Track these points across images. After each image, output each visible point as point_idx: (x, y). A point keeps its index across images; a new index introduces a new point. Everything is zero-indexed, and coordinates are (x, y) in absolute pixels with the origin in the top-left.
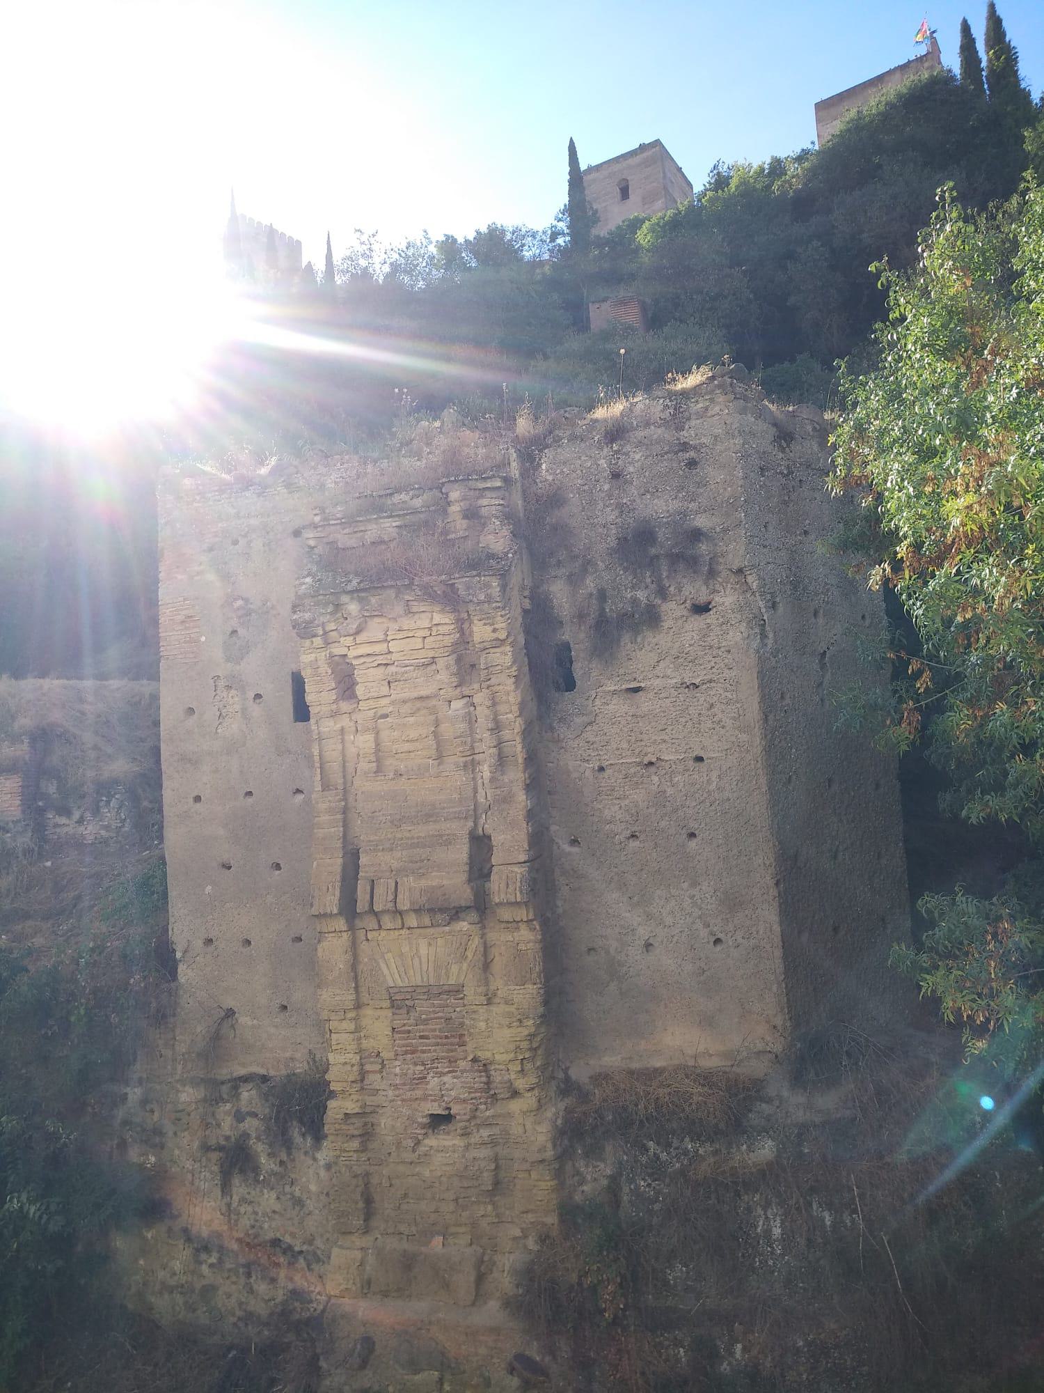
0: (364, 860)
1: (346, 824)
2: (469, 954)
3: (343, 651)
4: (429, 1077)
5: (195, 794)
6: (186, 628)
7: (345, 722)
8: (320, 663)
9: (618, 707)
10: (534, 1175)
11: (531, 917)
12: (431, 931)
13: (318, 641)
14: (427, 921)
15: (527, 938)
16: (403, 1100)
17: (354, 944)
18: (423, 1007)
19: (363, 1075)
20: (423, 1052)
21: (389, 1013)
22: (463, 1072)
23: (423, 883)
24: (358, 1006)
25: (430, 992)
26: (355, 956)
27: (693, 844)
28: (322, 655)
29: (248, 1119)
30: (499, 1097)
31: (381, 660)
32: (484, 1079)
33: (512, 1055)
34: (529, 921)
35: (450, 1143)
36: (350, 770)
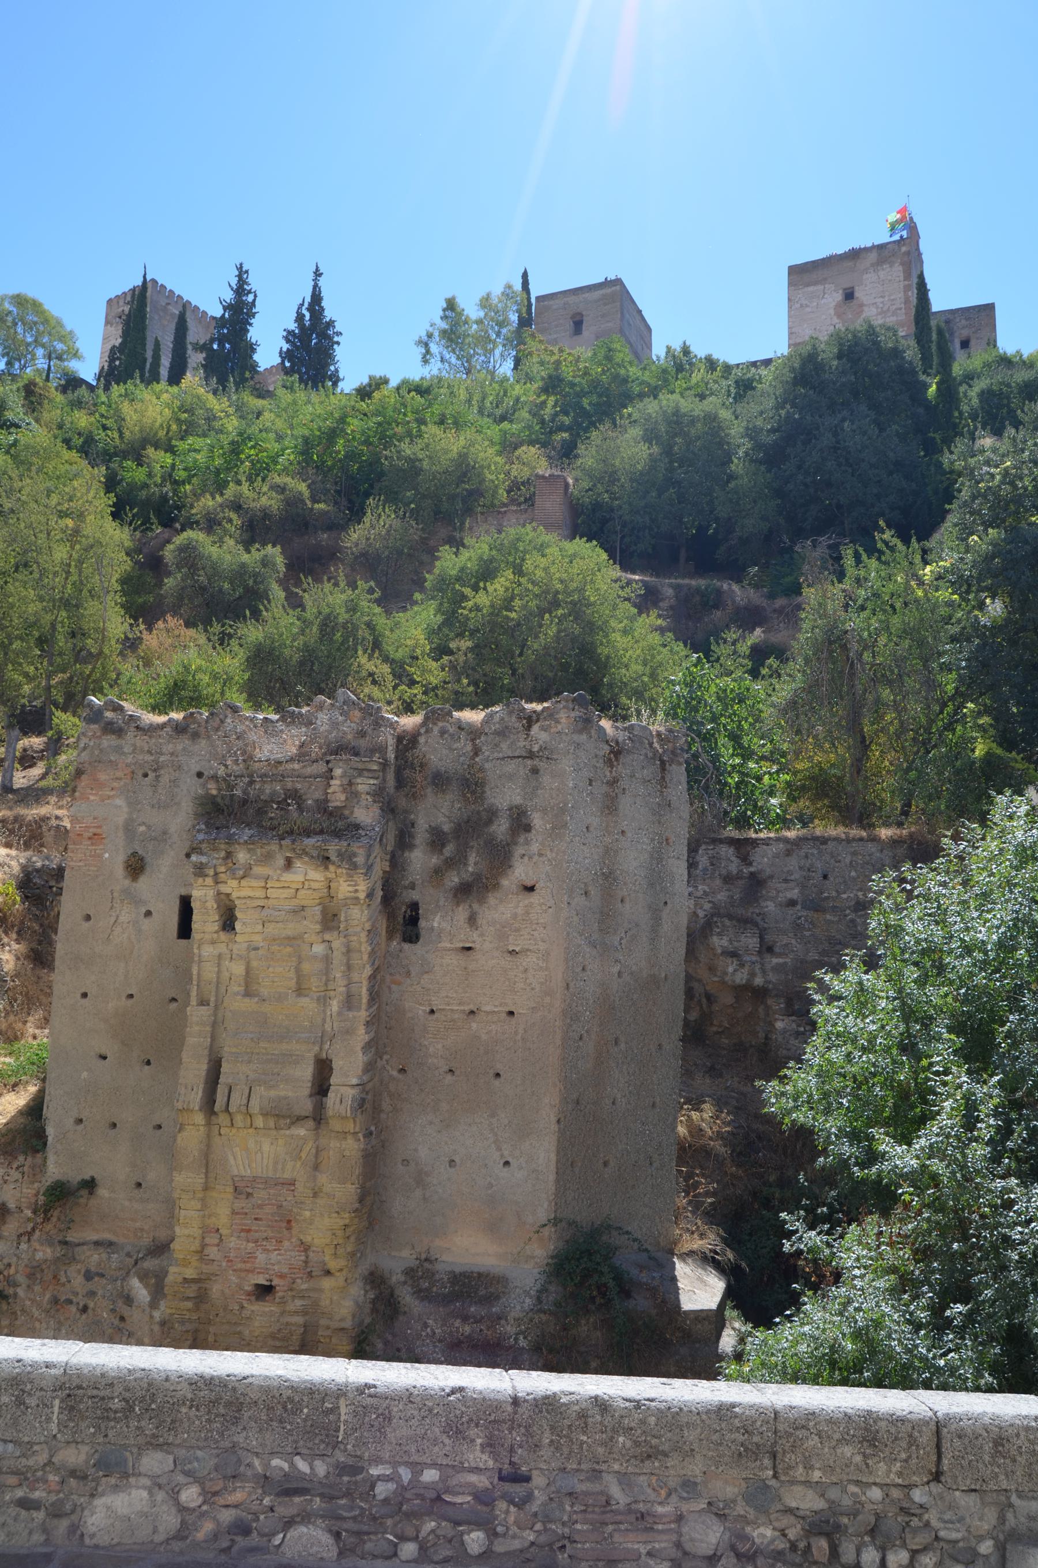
0: (225, 1068)
1: (213, 1038)
2: (303, 1155)
3: (228, 890)
4: (258, 1253)
5: (83, 990)
6: (92, 844)
7: (222, 948)
8: (208, 898)
9: (452, 961)
10: (334, 1340)
11: (357, 1130)
12: (274, 1132)
13: (209, 881)
14: (271, 1123)
15: (352, 1147)
16: (234, 1270)
17: (209, 1136)
18: (260, 1195)
19: (204, 1246)
20: (256, 1231)
21: (230, 1197)
22: (286, 1251)
23: (273, 1093)
24: (206, 1188)
25: (268, 1183)
26: (209, 1146)
27: (497, 1083)
28: (211, 893)
29: (96, 1279)
30: (314, 1274)
31: (261, 903)
32: (303, 1258)
33: (328, 1241)
34: (355, 1133)
35: (267, 1309)
36: (223, 990)
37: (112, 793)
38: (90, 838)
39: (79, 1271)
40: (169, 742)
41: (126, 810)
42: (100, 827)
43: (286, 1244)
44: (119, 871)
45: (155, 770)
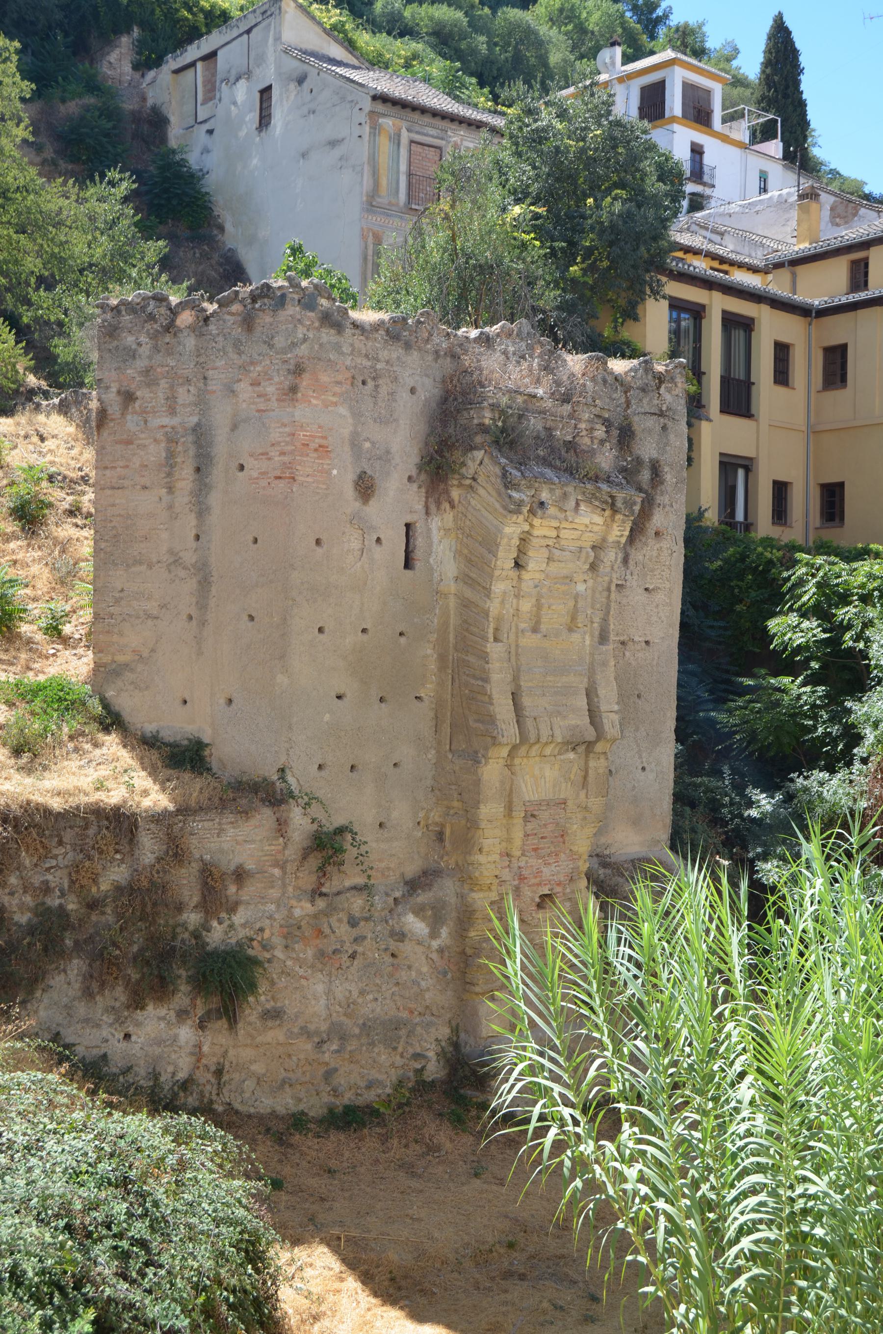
6: (318, 458)
18: (544, 815)
29: (362, 923)
37: (334, 399)
38: (316, 450)
39: (340, 920)
40: (384, 348)
41: (350, 421)
42: (325, 438)
43: (562, 855)
44: (349, 491)
45: (374, 379)
